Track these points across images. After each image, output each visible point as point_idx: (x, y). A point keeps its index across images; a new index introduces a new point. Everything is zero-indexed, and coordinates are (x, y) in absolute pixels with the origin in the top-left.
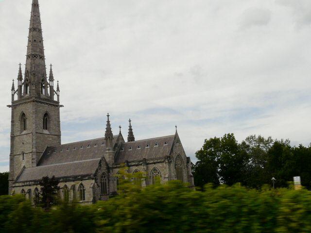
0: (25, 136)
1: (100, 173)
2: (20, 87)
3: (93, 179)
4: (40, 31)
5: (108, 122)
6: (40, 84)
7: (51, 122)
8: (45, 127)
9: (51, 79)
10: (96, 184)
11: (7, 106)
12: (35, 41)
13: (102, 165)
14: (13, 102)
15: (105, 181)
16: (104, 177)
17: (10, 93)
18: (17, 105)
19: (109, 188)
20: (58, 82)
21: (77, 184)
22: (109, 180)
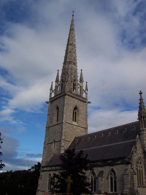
0: (57, 126)
2: (56, 87)
5: (141, 99)
6: (72, 83)
7: (80, 115)
8: (75, 119)
9: (81, 80)
10: (132, 170)
11: (46, 102)
13: (138, 148)
14: (51, 98)
15: (141, 169)
16: (140, 163)
18: (53, 101)
20: (87, 82)
21: (107, 170)
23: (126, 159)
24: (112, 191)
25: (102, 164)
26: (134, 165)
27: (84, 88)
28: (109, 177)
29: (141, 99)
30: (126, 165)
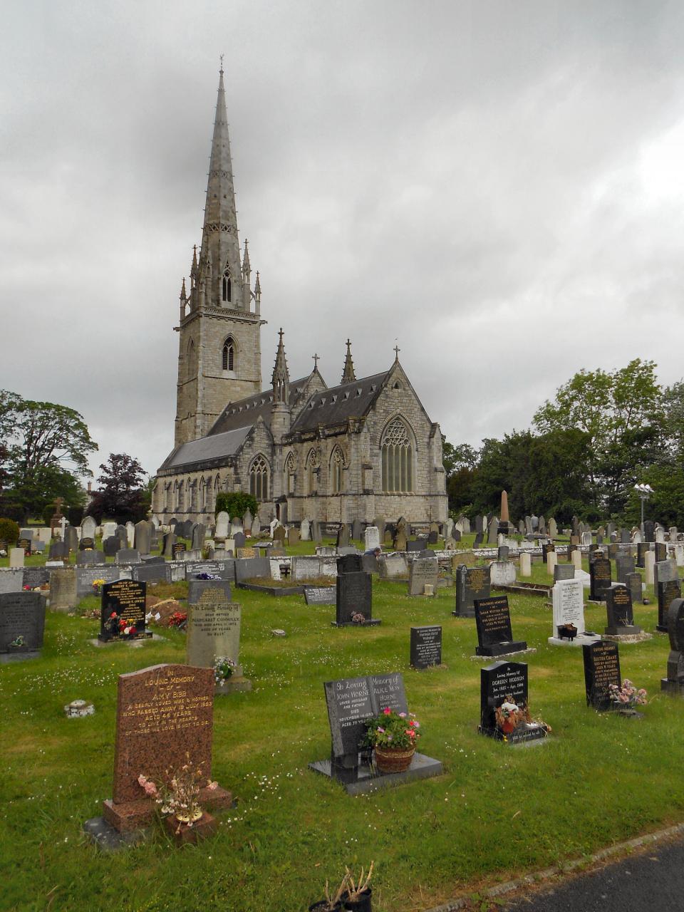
0: (192, 383)
1: (248, 455)
4: (228, 176)
7: (241, 355)
9: (247, 269)
11: (174, 329)
12: (215, 196)
13: (256, 439)
15: (262, 473)
16: (262, 464)
17: (177, 303)
22: (273, 471)
26: (244, 468)
27: (252, 289)
29: (281, 346)
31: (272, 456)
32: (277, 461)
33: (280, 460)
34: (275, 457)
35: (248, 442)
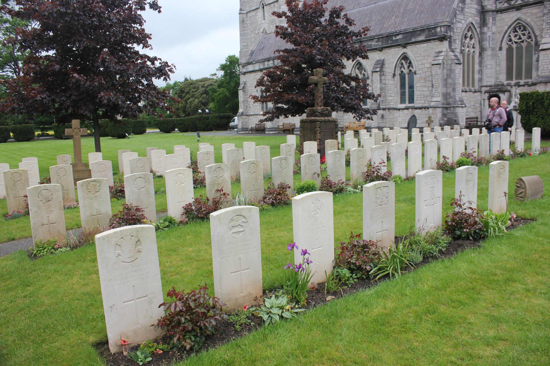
3: (442, 39)
10: (451, 53)
16: (471, 38)
19: (481, 72)
23: (438, 30)
24: (403, 101)
25: (380, 43)
28: (398, 72)
30: (438, 43)
31: (481, 28)
32: (489, 34)
33: (493, 33)
34: (485, 29)
35: (460, 5)
